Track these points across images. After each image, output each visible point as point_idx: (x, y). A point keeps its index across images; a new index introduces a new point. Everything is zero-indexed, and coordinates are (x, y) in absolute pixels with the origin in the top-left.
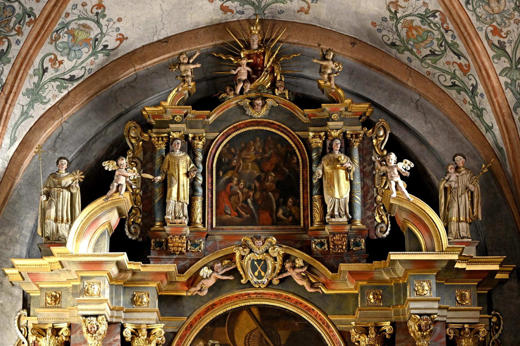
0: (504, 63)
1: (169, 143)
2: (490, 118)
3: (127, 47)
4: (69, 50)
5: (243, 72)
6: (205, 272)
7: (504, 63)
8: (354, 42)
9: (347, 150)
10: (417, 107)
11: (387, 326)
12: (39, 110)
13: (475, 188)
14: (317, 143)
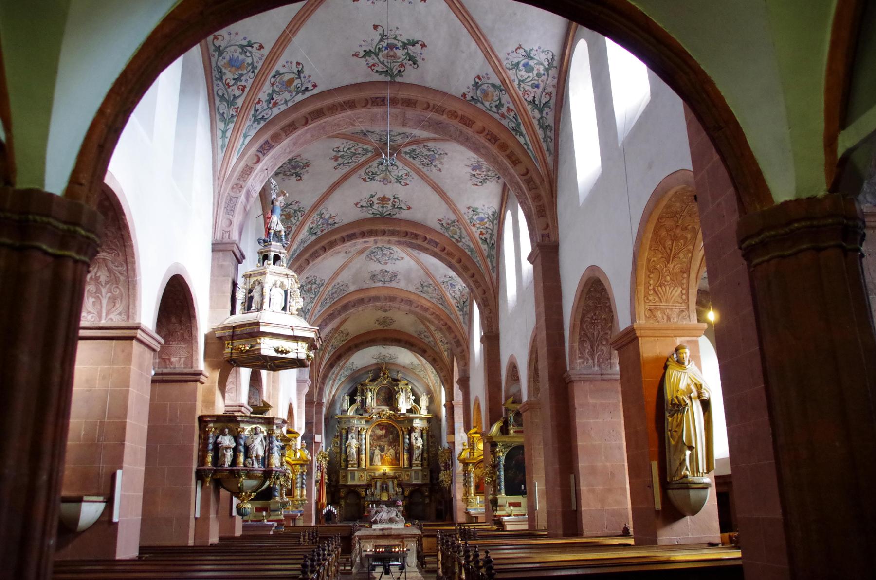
0: (433, 375)
1: (367, 389)
2: (431, 384)
3: (357, 369)
4: (346, 371)
5: (382, 374)
6: (374, 416)
7: (433, 375)
8: (404, 367)
9: (402, 392)
10: (417, 381)
11: (409, 428)
12: (340, 382)
13: (427, 400)
14: (397, 389)
